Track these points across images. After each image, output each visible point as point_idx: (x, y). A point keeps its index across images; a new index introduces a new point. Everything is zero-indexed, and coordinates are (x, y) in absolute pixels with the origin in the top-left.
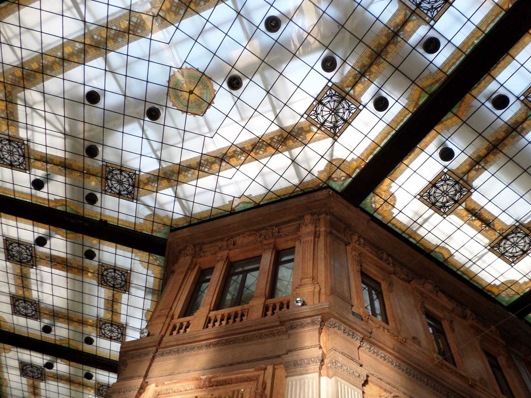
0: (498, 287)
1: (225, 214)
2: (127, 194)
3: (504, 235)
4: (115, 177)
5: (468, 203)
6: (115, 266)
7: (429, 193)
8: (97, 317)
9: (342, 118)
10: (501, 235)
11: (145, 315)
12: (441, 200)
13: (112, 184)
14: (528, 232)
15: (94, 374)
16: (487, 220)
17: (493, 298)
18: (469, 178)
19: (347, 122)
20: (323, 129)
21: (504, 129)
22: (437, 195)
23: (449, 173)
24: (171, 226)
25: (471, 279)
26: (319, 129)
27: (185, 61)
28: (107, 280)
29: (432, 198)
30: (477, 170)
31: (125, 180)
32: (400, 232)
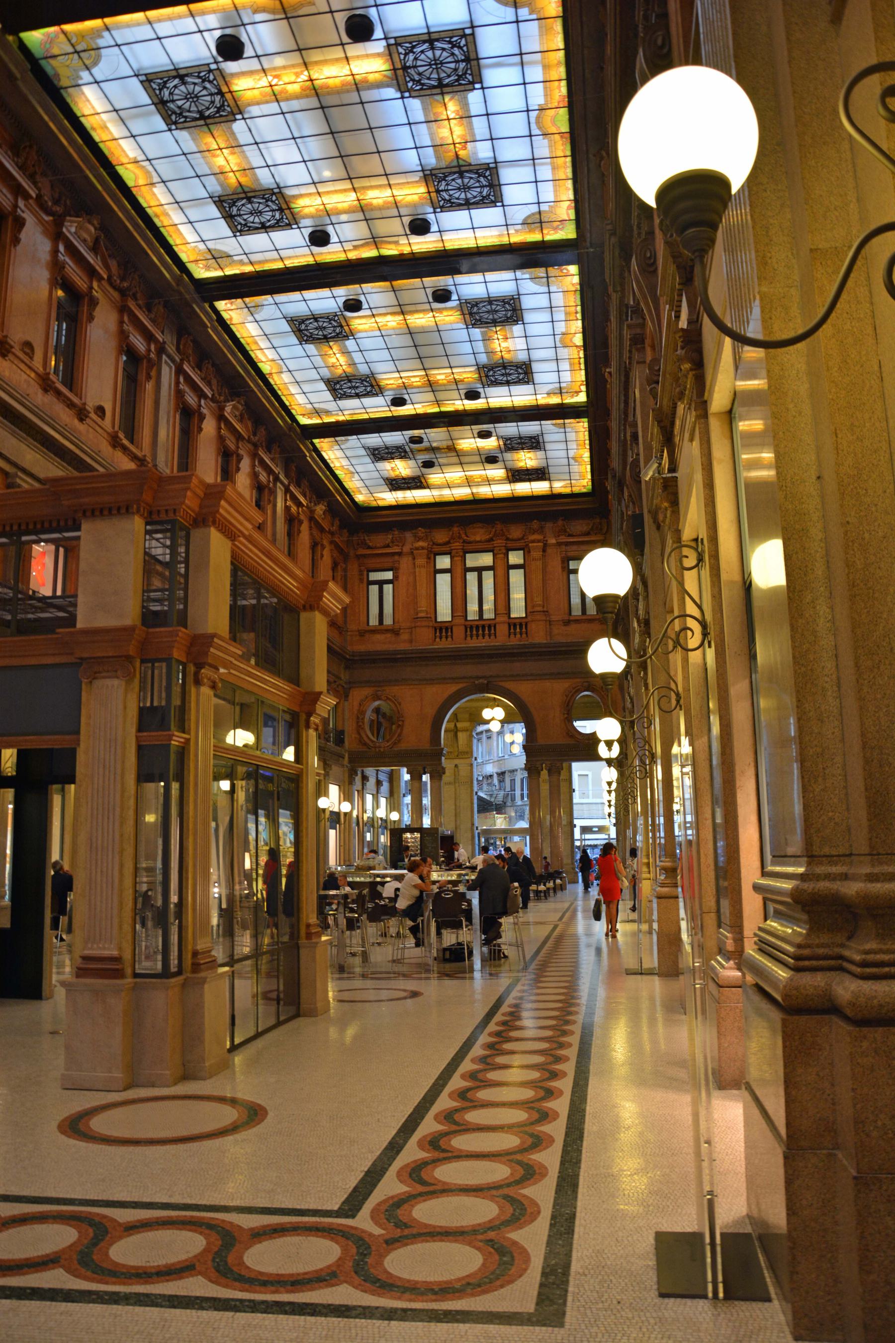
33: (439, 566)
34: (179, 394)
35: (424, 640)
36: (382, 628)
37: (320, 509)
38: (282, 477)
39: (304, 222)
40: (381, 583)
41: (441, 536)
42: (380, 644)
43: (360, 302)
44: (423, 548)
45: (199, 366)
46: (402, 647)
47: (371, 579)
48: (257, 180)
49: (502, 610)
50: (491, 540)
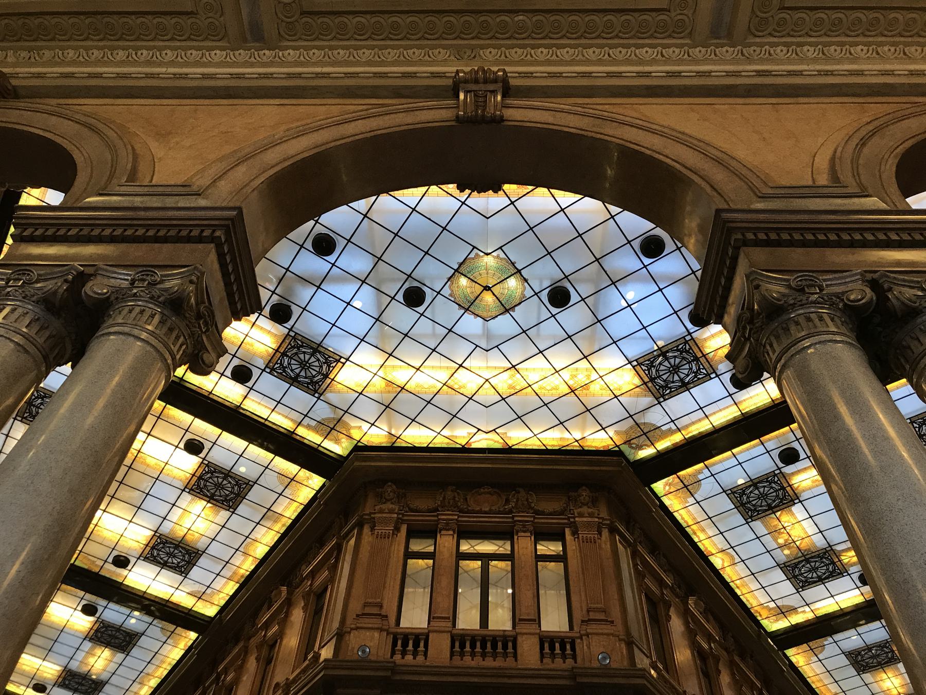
0: (770, 609)
1: (453, 446)
2: (308, 384)
4: (302, 356)
6: (230, 471)
8: (156, 532)
9: (682, 380)
11: (247, 545)
12: (754, 503)
13: (289, 364)
15: (100, 609)
17: (758, 621)
19: (685, 386)
20: (650, 385)
24: (359, 441)
26: (645, 383)
27: (500, 248)
28: (205, 486)
31: (317, 364)
32: (684, 525)
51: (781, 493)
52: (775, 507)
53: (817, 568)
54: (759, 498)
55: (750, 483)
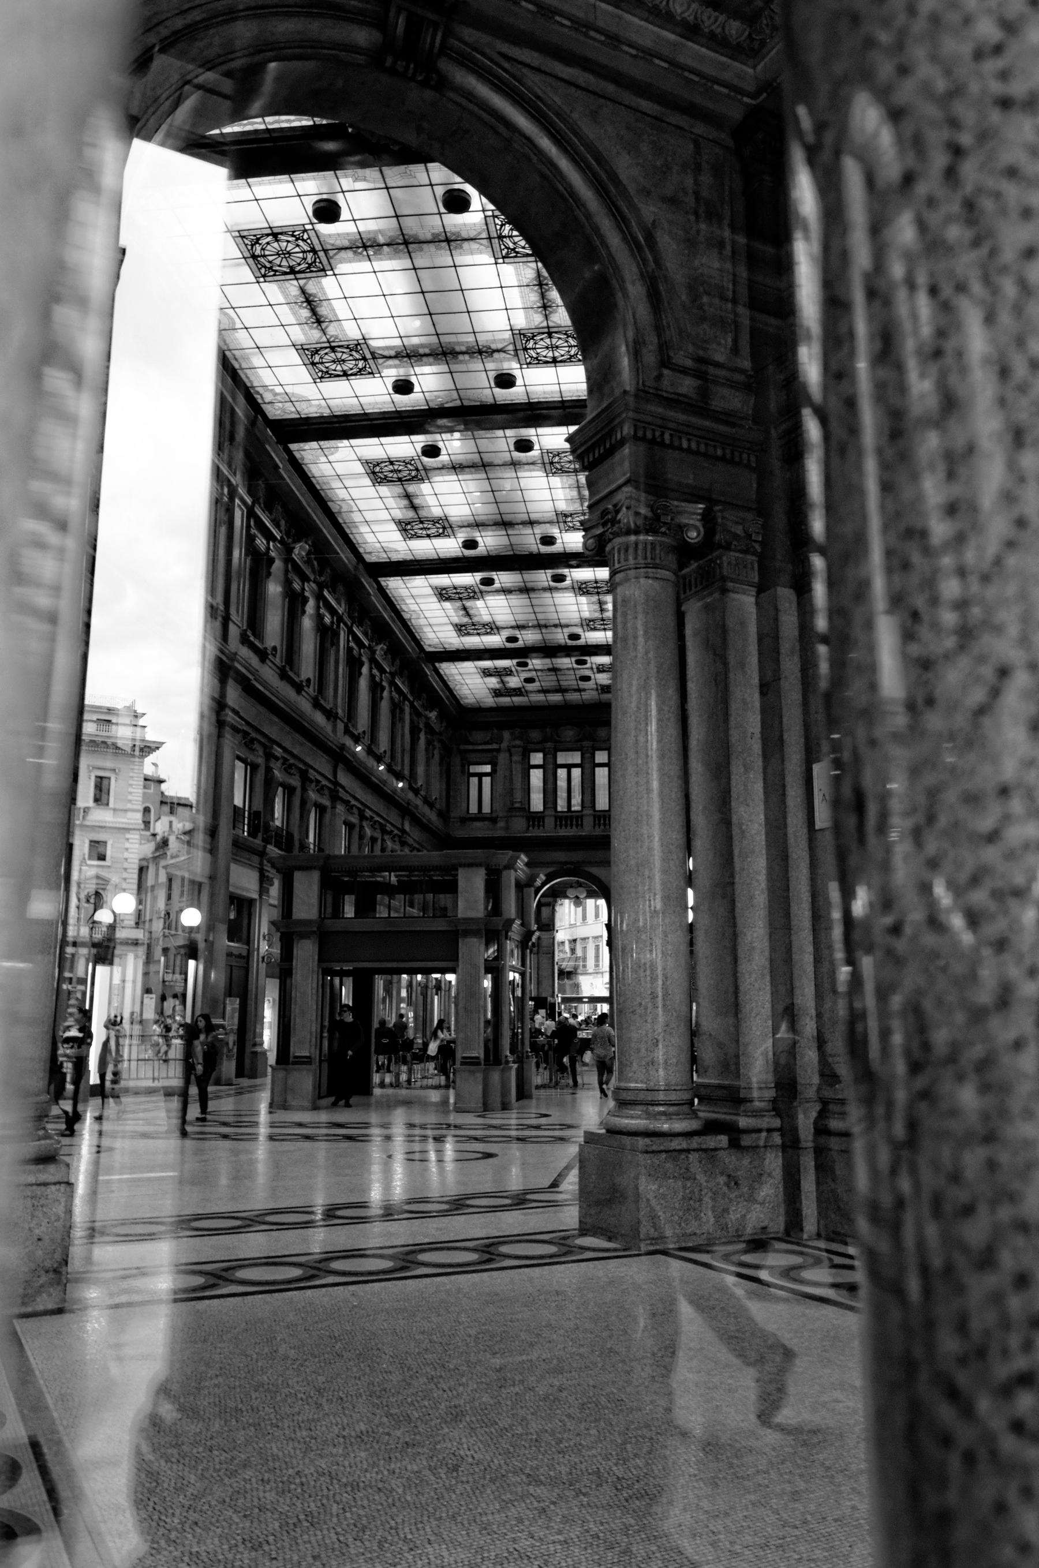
0: (276, 394)
3: (333, 344)
5: (310, 282)
7: (258, 239)
10: (329, 342)
12: (271, 258)
14: (368, 356)
16: (321, 316)
17: (258, 404)
18: (337, 257)
21: (436, 231)
22: (269, 247)
23: (312, 234)
25: (242, 369)
29: (258, 248)
30: (355, 252)
33: (533, 762)
34: (349, 650)
35: (519, 826)
36: (480, 817)
37: (433, 715)
38: (409, 696)
39: (459, 535)
40: (480, 776)
41: (535, 735)
42: (479, 831)
43: (493, 580)
44: (519, 747)
45: (360, 624)
46: (499, 833)
47: (471, 771)
48: (343, 330)
49: (588, 803)
50: (580, 740)
51: (310, 256)
52: (300, 272)
53: (344, 361)
54: (278, 254)
55: (269, 231)
